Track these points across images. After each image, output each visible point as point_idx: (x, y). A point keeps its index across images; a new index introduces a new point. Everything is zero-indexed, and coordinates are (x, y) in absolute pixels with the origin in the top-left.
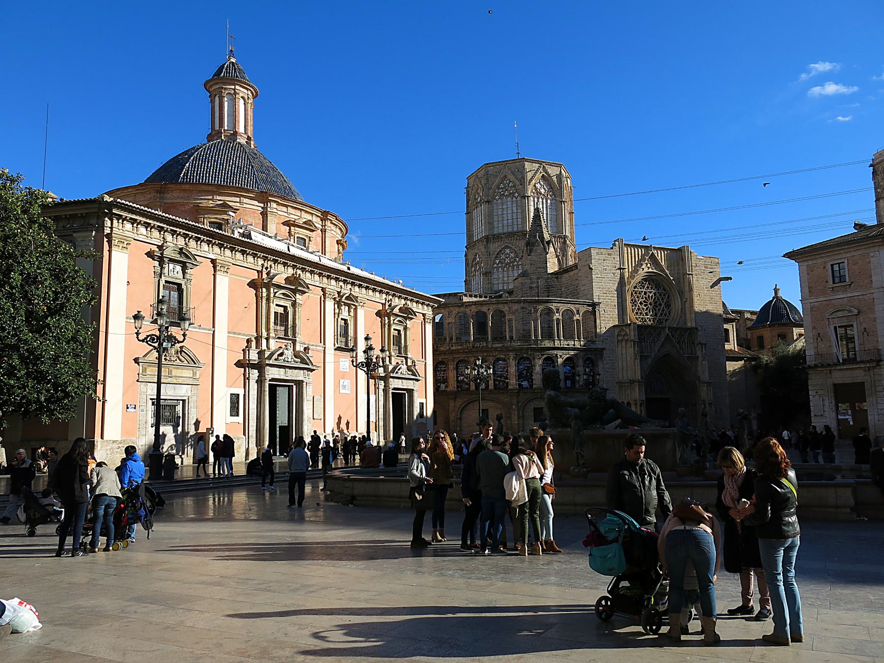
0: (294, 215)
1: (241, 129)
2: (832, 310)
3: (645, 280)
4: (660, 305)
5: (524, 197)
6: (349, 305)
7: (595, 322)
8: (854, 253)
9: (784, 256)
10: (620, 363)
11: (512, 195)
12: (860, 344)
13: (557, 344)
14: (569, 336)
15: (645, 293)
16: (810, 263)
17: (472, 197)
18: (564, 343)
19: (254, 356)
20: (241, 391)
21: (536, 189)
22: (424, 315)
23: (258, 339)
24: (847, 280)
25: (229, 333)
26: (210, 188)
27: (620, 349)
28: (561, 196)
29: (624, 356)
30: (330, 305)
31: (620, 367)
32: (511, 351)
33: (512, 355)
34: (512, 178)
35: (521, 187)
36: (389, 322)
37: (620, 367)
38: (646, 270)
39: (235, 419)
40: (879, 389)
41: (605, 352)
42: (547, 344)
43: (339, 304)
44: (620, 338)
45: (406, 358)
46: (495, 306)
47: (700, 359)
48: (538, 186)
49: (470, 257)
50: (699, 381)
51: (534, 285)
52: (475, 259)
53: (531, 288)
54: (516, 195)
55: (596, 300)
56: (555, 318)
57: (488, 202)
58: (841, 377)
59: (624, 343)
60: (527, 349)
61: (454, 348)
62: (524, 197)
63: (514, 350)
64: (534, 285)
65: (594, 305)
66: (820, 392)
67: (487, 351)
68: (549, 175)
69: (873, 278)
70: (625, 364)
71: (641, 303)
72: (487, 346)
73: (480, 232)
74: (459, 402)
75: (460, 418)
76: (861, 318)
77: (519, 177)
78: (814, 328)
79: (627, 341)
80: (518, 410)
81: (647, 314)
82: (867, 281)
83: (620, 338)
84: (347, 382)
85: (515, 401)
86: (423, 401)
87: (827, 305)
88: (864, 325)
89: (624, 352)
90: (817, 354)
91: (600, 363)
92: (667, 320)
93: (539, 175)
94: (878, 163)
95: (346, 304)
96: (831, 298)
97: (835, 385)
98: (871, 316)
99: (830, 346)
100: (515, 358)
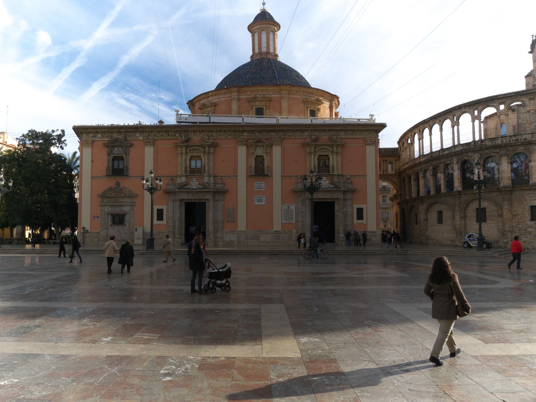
33: (455, 160)
61: (421, 160)
100: (457, 162)
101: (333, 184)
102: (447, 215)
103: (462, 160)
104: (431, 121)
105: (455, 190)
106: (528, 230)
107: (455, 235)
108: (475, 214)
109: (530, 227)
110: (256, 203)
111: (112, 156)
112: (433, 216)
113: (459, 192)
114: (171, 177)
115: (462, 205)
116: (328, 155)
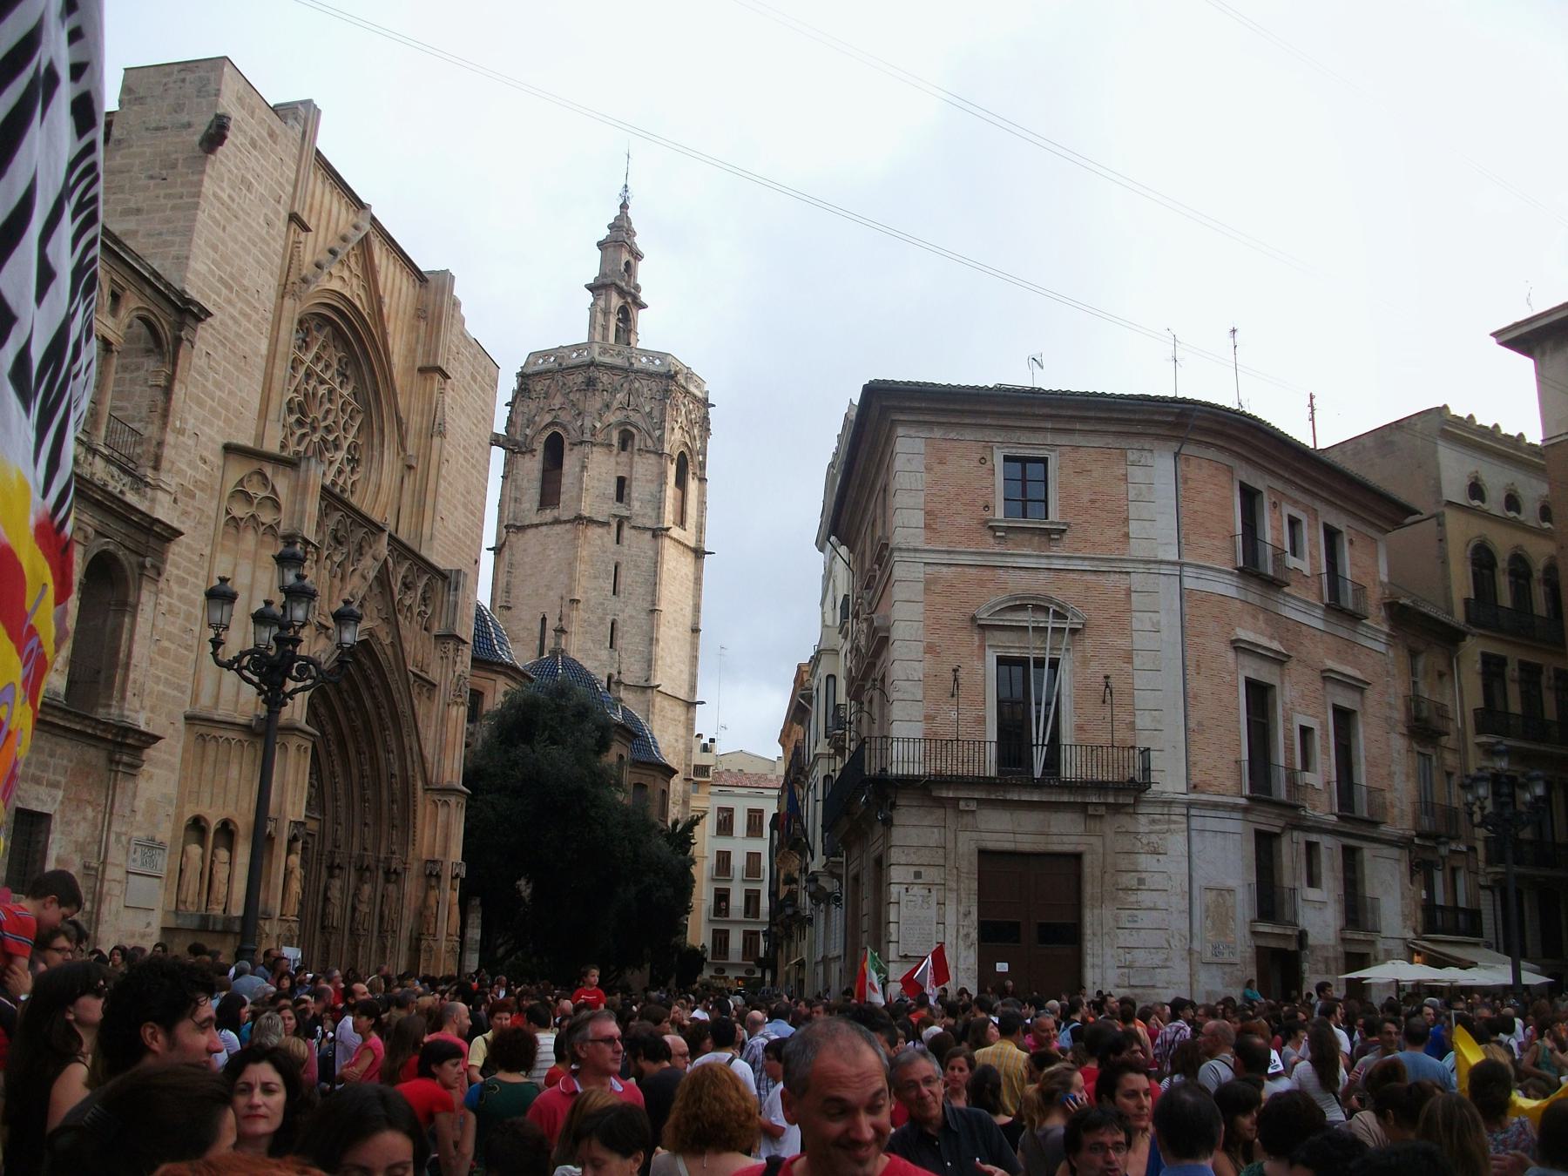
2: (998, 598)
4: (337, 447)
8: (1078, 440)
12: (1080, 728)
16: (938, 433)
24: (1054, 515)
38: (336, 285)
40: (1129, 880)
41: (176, 551)
44: (240, 510)
50: (426, 781)
58: (1007, 830)
59: (250, 539)
65: (189, 312)
66: (930, 875)
69: (1133, 527)
76: (1088, 643)
78: (930, 649)
79: (272, 529)
82: (1111, 533)
83: (240, 510)
87: (981, 583)
88: (1096, 670)
90: (934, 742)
91: (146, 596)
94: (539, 374)
96: (998, 561)
97: (984, 854)
98: (1121, 642)
99: (981, 720)
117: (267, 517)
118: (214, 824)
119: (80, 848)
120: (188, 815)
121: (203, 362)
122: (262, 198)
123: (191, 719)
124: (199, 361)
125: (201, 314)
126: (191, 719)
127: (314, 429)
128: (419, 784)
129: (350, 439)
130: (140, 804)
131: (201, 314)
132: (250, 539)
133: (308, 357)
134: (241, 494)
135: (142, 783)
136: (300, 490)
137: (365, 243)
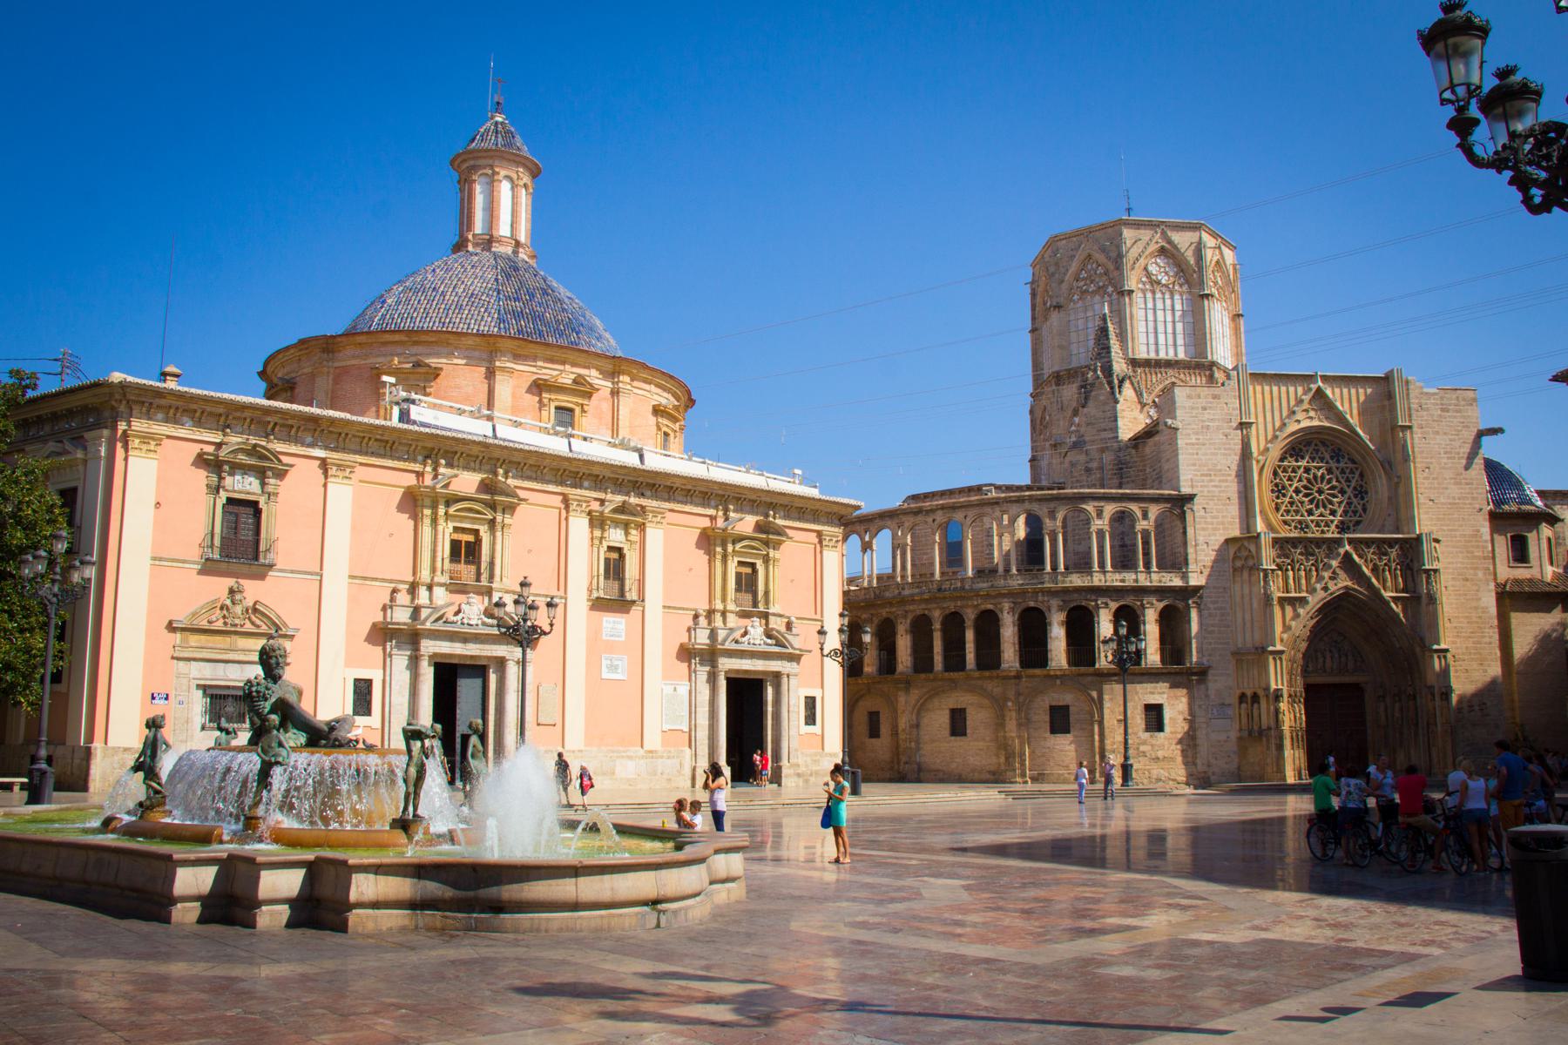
0: (548, 371)
1: (504, 230)
3: (1309, 444)
5: (1122, 293)
6: (626, 526)
7: (1185, 533)
9: (1555, 379)
10: (1239, 615)
11: (1101, 290)
13: (1097, 580)
14: (1124, 561)
15: (1307, 470)
17: (1039, 299)
18: (1115, 579)
19: (401, 616)
20: (376, 676)
21: (1148, 275)
22: (819, 534)
23: (413, 589)
25: (351, 577)
26: (397, 337)
27: (1237, 587)
28: (1201, 283)
29: (1247, 599)
30: (579, 526)
31: (1239, 620)
32: (1004, 596)
33: (1006, 606)
34: (1101, 258)
35: (1116, 273)
36: (725, 550)
37: (1239, 620)
38: (1305, 424)
39: (811, 729)
42: (1076, 580)
43: (598, 522)
45: (765, 616)
46: (975, 511)
47: (1424, 600)
48: (1153, 269)
49: (1038, 414)
51: (1094, 465)
52: (1043, 418)
53: (1088, 470)
54: (1110, 289)
55: (1185, 490)
56: (1093, 528)
57: (1058, 307)
59: (1246, 574)
60: (1036, 592)
61: (906, 592)
62: (1122, 293)
63: (1011, 594)
64: (1094, 465)
67: (962, 598)
68: (1175, 247)
70: (1248, 617)
71: (1297, 491)
72: (963, 588)
73: (1048, 370)
74: (915, 694)
75: (918, 726)
77: (1113, 255)
79: (1251, 569)
80: (1019, 711)
81: (1310, 513)
83: (1239, 564)
84: (622, 662)
85: (1011, 694)
86: (816, 693)
89: (1246, 591)
92: (1358, 523)
93: (1153, 247)
95: (616, 523)
100: (1012, 610)
101: (769, 636)
102: (977, 718)
103: (1024, 606)
104: (940, 513)
105: (1004, 666)
106: (1142, 748)
107: (1002, 760)
108: (1047, 718)
109: (1144, 743)
110: (605, 675)
111: (223, 495)
112: (938, 720)
113: (1018, 677)
114: (391, 581)
115: (1021, 699)
116: (256, 503)
117: (1251, 563)
118: (1249, 693)
119: (1181, 713)
120: (1238, 692)
121: (1202, 513)
122: (1218, 428)
123: (1233, 654)
124: (1199, 513)
125: (1190, 498)
126: (1233, 654)
127: (1320, 492)
128: (1418, 649)
129: (1353, 484)
130: (1212, 693)
131: (1190, 498)
132: (1246, 574)
133: (1303, 463)
134: (1235, 557)
135: (1211, 685)
136: (1258, 548)
137: (1319, 393)
